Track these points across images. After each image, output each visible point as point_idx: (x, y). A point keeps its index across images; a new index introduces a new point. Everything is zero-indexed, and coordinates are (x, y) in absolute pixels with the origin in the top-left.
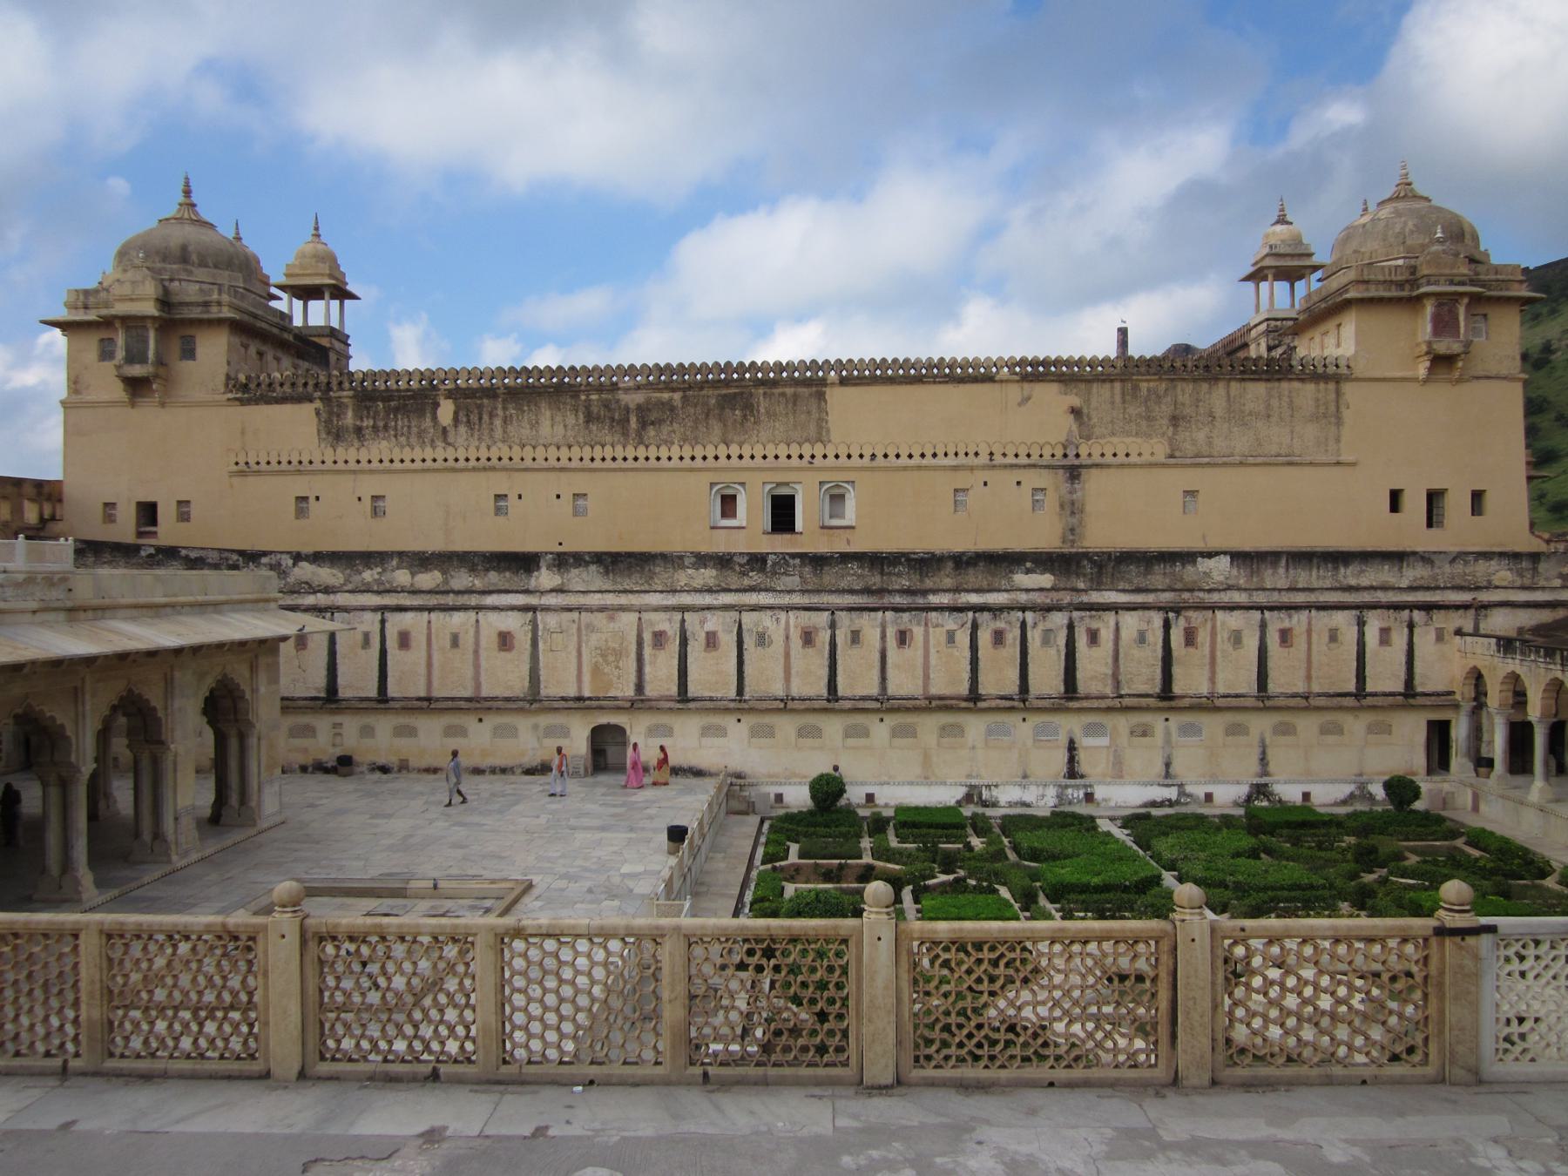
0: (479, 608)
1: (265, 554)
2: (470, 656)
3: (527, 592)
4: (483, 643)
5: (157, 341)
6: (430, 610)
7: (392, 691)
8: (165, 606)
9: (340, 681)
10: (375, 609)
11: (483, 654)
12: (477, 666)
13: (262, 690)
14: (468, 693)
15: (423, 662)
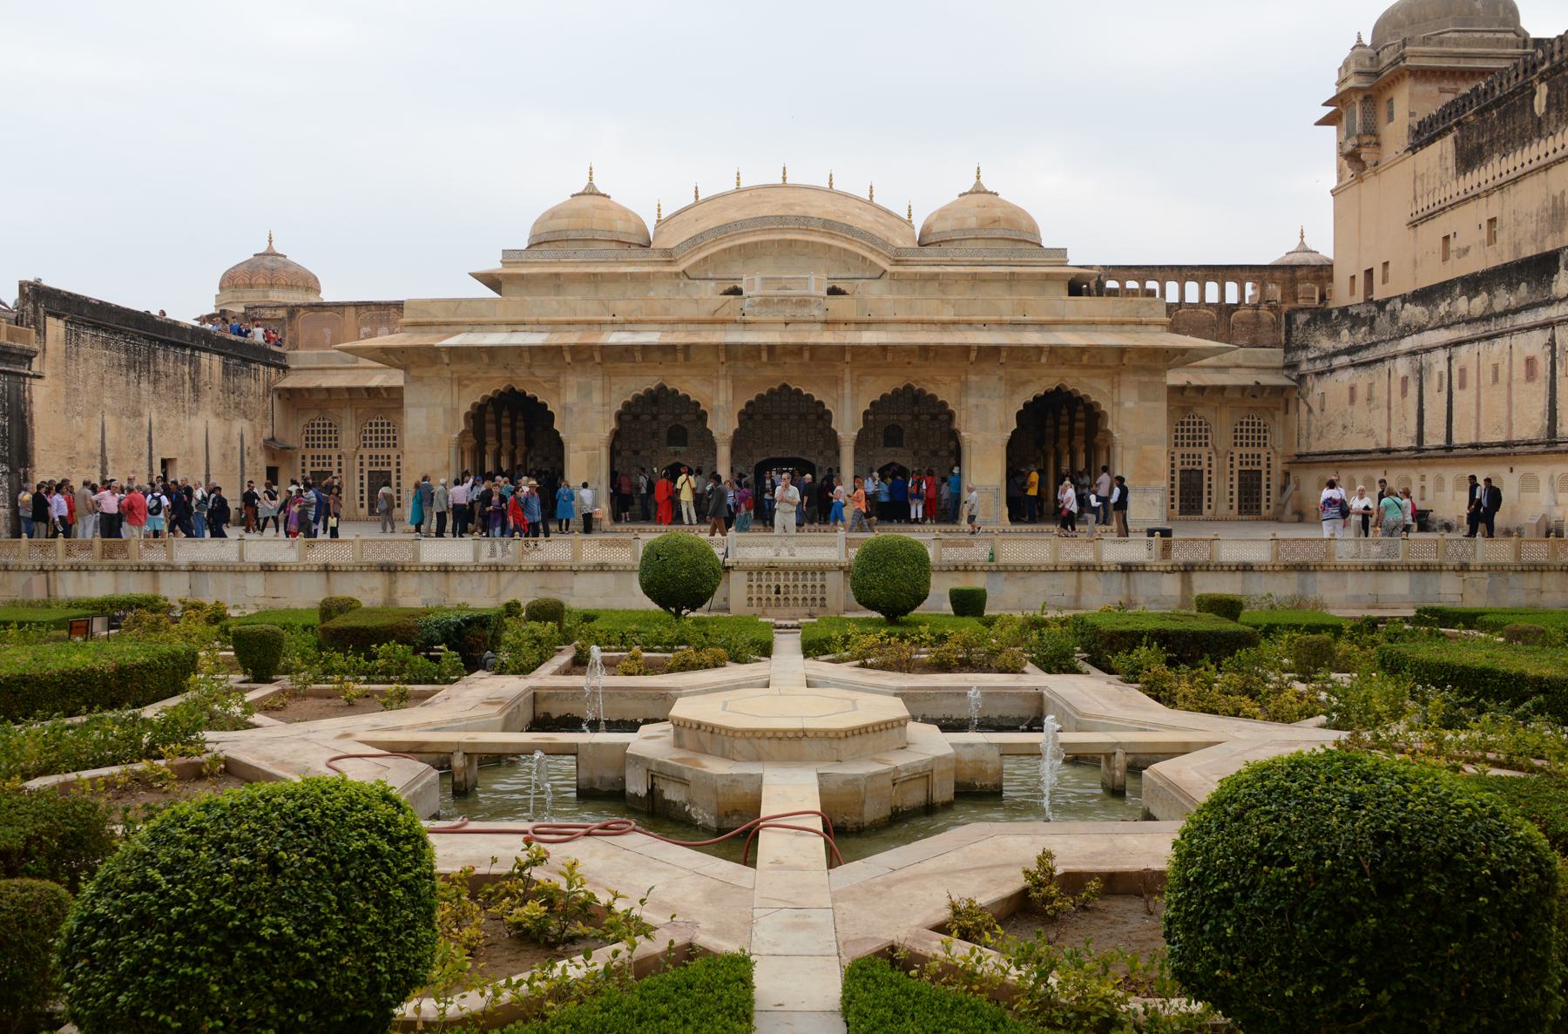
0: (1511, 332)
1: (1388, 300)
2: (1505, 392)
3: (1549, 303)
4: (1515, 375)
5: (1364, 112)
6: (1479, 340)
7: (1456, 441)
8: (954, 323)
9: (1426, 430)
10: (1445, 346)
11: (1514, 386)
12: (1510, 402)
13: (1129, 404)
14: (1502, 438)
15: (1474, 401)
